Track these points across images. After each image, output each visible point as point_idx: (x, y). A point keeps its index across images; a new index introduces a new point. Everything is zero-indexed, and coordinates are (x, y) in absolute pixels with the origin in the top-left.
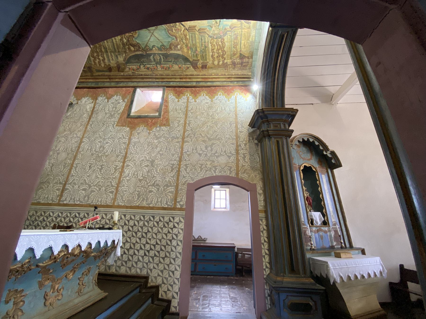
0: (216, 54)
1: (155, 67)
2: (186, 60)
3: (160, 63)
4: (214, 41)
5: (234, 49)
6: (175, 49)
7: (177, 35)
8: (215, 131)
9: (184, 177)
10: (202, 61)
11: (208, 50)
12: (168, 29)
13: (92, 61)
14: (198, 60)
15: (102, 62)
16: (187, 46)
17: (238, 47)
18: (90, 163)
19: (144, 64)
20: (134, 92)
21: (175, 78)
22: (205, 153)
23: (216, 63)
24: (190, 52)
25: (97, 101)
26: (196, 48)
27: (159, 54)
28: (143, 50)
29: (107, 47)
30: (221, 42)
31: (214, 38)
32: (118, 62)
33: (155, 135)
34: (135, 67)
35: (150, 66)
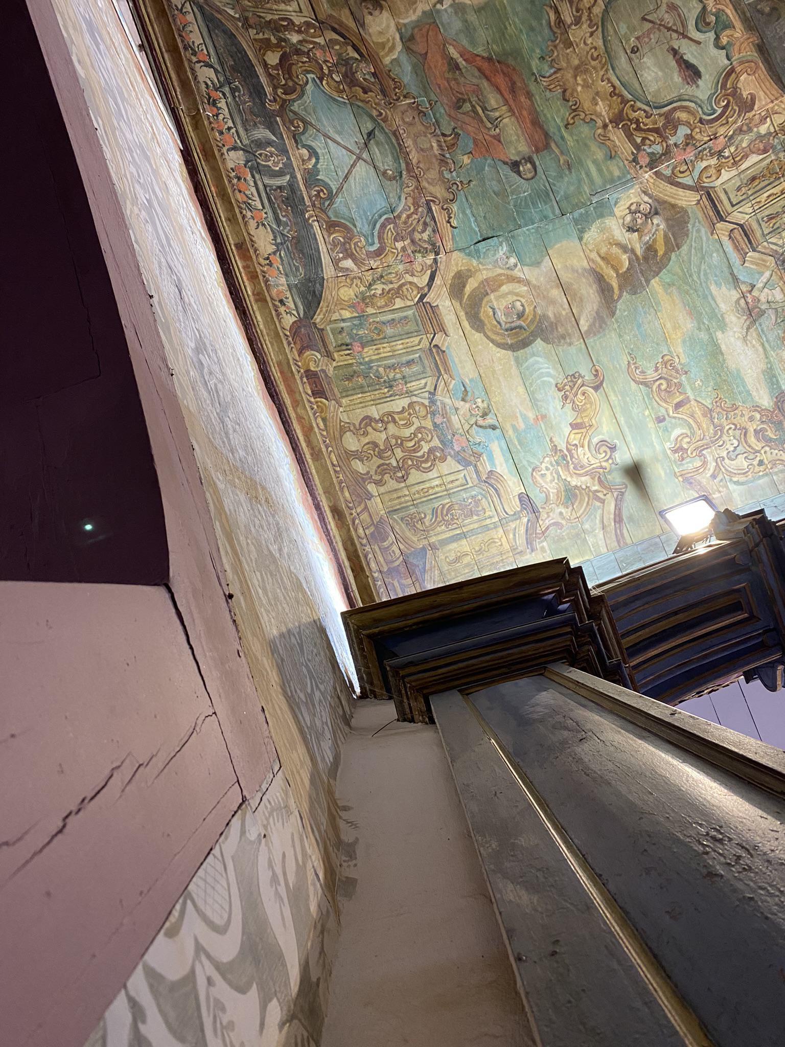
0: (383, 436)
2: (311, 294)
4: (425, 417)
5: (430, 512)
6: (335, 244)
7: (390, 259)
10: (331, 372)
11: (383, 399)
12: (400, 222)
14: (329, 355)
16: (365, 299)
17: (442, 533)
19: (226, 89)
23: (352, 443)
24: (347, 314)
26: (372, 342)
28: (284, 104)
30: (431, 451)
31: (433, 414)
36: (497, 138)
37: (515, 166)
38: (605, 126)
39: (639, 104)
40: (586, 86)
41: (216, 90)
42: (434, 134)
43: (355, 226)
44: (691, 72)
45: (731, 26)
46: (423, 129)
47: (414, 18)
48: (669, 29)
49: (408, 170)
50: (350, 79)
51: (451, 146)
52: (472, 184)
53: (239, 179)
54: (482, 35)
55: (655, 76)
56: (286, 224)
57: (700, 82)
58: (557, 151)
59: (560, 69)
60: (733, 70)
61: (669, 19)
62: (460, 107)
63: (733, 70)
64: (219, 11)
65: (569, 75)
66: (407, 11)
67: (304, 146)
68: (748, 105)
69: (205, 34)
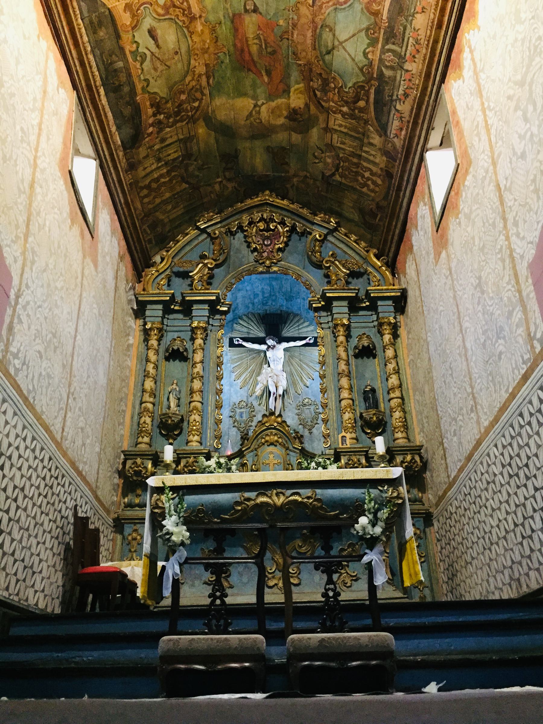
1: (407, 76)
3: (402, 58)
8: (523, 40)
9: (522, 257)
13: (369, 193)
15: (374, 178)
18: (443, 375)
19: (395, 97)
20: (425, 167)
21: (436, 41)
22: (529, 134)
25: (415, 248)
27: (383, 52)
28: (368, 81)
29: (351, 149)
32: (380, 149)
33: (465, 215)
34: (396, 124)
35: (401, 88)
36: (259, 28)
37: (256, 10)
38: (200, 17)
39: (181, 24)
40: (204, 42)
41: (400, 100)
42: (292, 40)
43: (362, 9)
44: (152, 33)
45: (131, 52)
46: (298, 46)
47: (280, 101)
48: (159, 59)
49: (316, 28)
50: (326, 83)
51: (287, 32)
52: (283, 8)
53: (414, 57)
54: (248, 82)
55: (169, 36)
56: (401, 25)
57: (149, 27)
58: (230, 11)
59: (215, 54)
60: (133, 29)
61: (158, 64)
62: (273, 51)
63: (133, 29)
64: (377, 131)
65: (212, 49)
66: (281, 104)
67: (368, 59)
68: (128, 7)
69: (390, 123)
